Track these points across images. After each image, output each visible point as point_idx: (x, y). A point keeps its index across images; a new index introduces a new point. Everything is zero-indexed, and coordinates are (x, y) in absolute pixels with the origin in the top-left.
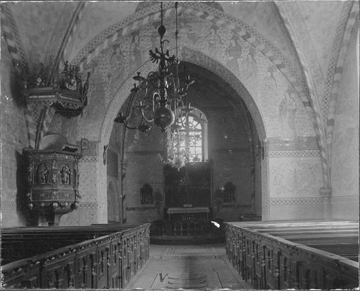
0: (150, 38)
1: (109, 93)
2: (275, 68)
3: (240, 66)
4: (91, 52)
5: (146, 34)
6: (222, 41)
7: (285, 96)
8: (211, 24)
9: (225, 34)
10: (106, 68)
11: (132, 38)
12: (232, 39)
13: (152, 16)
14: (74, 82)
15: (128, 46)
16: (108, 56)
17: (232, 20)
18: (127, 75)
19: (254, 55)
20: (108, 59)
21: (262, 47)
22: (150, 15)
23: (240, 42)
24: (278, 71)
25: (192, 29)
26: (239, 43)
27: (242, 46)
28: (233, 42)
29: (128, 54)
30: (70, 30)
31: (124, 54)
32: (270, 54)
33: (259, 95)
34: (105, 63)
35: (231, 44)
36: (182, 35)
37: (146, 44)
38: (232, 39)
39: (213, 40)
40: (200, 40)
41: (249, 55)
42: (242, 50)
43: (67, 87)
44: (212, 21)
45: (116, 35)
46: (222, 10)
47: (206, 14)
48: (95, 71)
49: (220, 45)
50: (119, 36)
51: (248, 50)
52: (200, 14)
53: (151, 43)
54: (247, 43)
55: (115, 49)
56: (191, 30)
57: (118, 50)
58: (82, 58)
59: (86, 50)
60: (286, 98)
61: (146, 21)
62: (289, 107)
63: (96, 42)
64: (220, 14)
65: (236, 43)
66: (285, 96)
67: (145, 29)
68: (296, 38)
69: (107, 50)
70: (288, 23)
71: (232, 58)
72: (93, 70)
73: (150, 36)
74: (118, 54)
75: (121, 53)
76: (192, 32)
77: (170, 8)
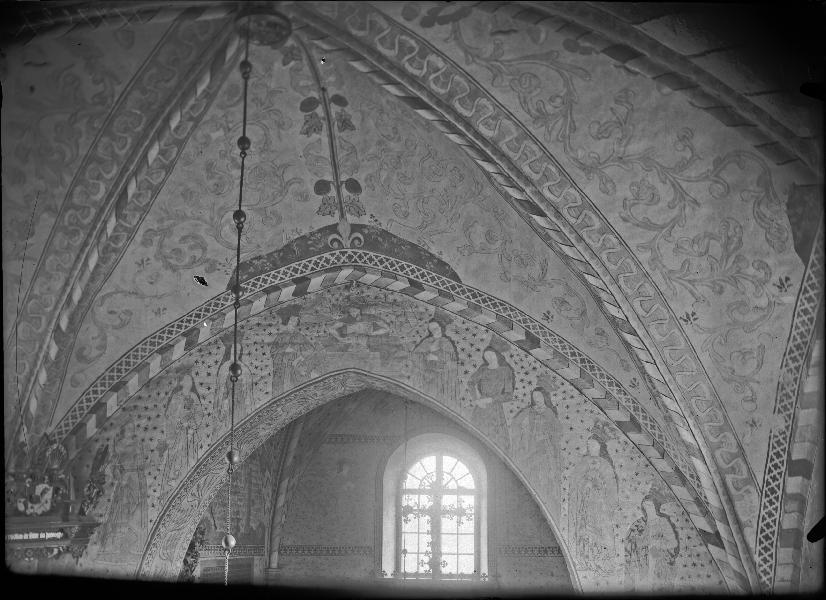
0: (267, 350)
1: (157, 494)
2: (612, 430)
3: (509, 423)
4: (115, 389)
5: (258, 339)
6: (462, 356)
7: (643, 510)
8: (432, 309)
9: (469, 336)
10: (155, 428)
11: (223, 348)
12: (490, 348)
13: (273, 295)
14: (44, 492)
15: (213, 371)
16: (162, 395)
17: (484, 301)
18: (206, 448)
19: (552, 393)
20: (160, 405)
21: (572, 373)
22: (267, 291)
23: (512, 356)
24: (623, 438)
25: (380, 323)
26: (508, 359)
27: (516, 368)
28: (491, 356)
29: (212, 390)
30: (41, 356)
31: (202, 391)
32: (595, 392)
33: (566, 505)
34: (153, 414)
35: (486, 363)
36: (352, 341)
37: (256, 363)
38: (490, 348)
39: (434, 353)
40: (402, 353)
41: (536, 394)
42: (518, 378)
43: (21, 507)
44: (431, 302)
45: (183, 342)
46: (455, 277)
47: (416, 286)
48: (128, 434)
49: (451, 365)
50: (189, 346)
51: (532, 377)
52: (402, 284)
53: (270, 362)
54: (531, 359)
55: (180, 379)
56: (376, 327)
57: (187, 382)
58: (92, 404)
59: (103, 385)
60: (646, 516)
61: (259, 304)
62: (655, 543)
63: (128, 364)
64: (453, 288)
65: (502, 361)
66: (643, 510)
67: (259, 324)
68: (662, 368)
69: (158, 381)
70: (634, 333)
71: (489, 400)
72: (123, 432)
73: (269, 344)
74: (186, 391)
75: (193, 389)
76: (381, 332)
77: (319, 273)
